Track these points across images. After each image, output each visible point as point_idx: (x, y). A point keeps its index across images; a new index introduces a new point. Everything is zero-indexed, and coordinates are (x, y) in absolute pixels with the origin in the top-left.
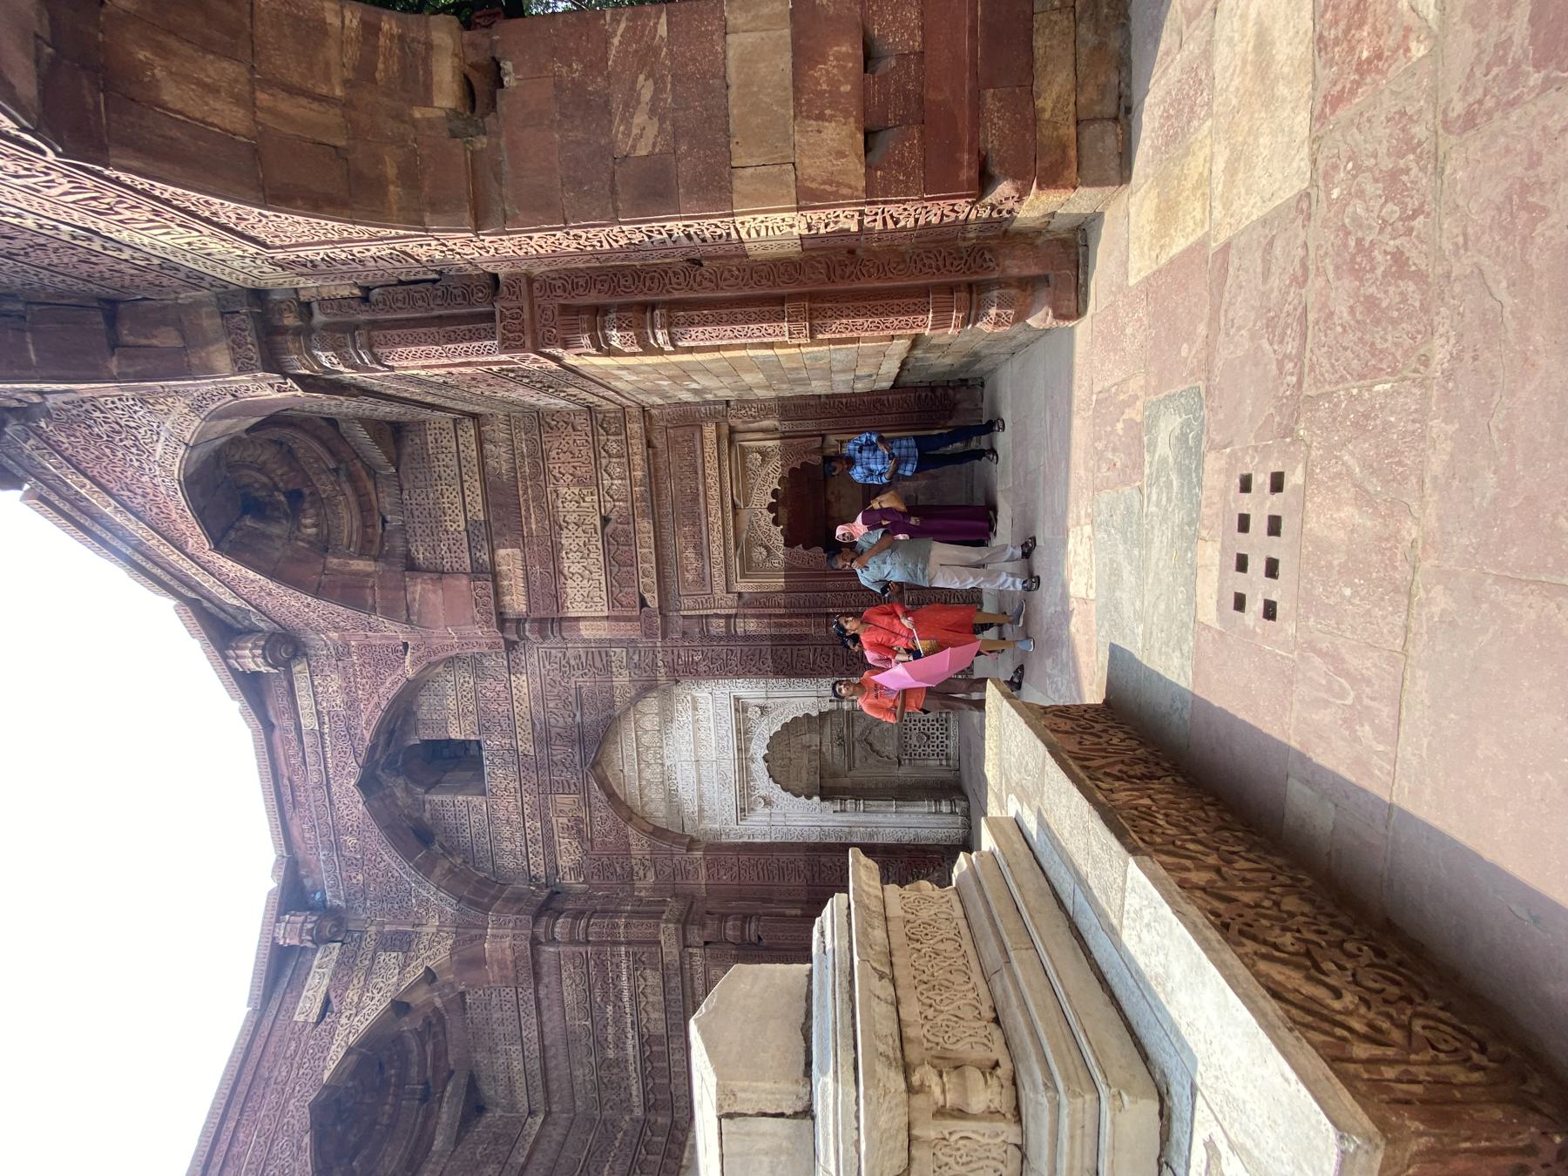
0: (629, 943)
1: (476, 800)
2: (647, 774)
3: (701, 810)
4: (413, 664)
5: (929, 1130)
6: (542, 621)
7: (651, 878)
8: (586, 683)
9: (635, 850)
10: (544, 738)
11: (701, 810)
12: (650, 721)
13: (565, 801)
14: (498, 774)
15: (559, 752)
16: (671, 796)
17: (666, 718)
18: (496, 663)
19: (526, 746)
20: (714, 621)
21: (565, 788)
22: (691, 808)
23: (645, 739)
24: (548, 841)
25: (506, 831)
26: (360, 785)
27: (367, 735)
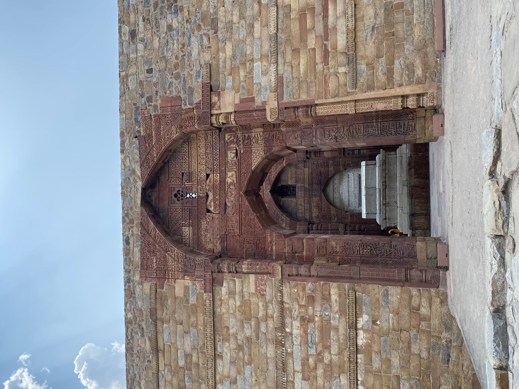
0: (331, 230)
1: (294, 200)
2: (335, 195)
3: (349, 204)
4: (285, 163)
5: (387, 156)
6: (316, 152)
7: (336, 219)
8: (322, 170)
9: (332, 212)
10: (311, 184)
11: (349, 204)
12: (336, 181)
13: (316, 199)
14: (299, 193)
15: (315, 187)
16: (341, 201)
17: (341, 180)
18: (301, 165)
19: (307, 186)
20: (355, 151)
21: (315, 196)
22: (346, 203)
23: (335, 186)
24: (310, 210)
25: (300, 207)
26: (270, 192)
27: (273, 180)
